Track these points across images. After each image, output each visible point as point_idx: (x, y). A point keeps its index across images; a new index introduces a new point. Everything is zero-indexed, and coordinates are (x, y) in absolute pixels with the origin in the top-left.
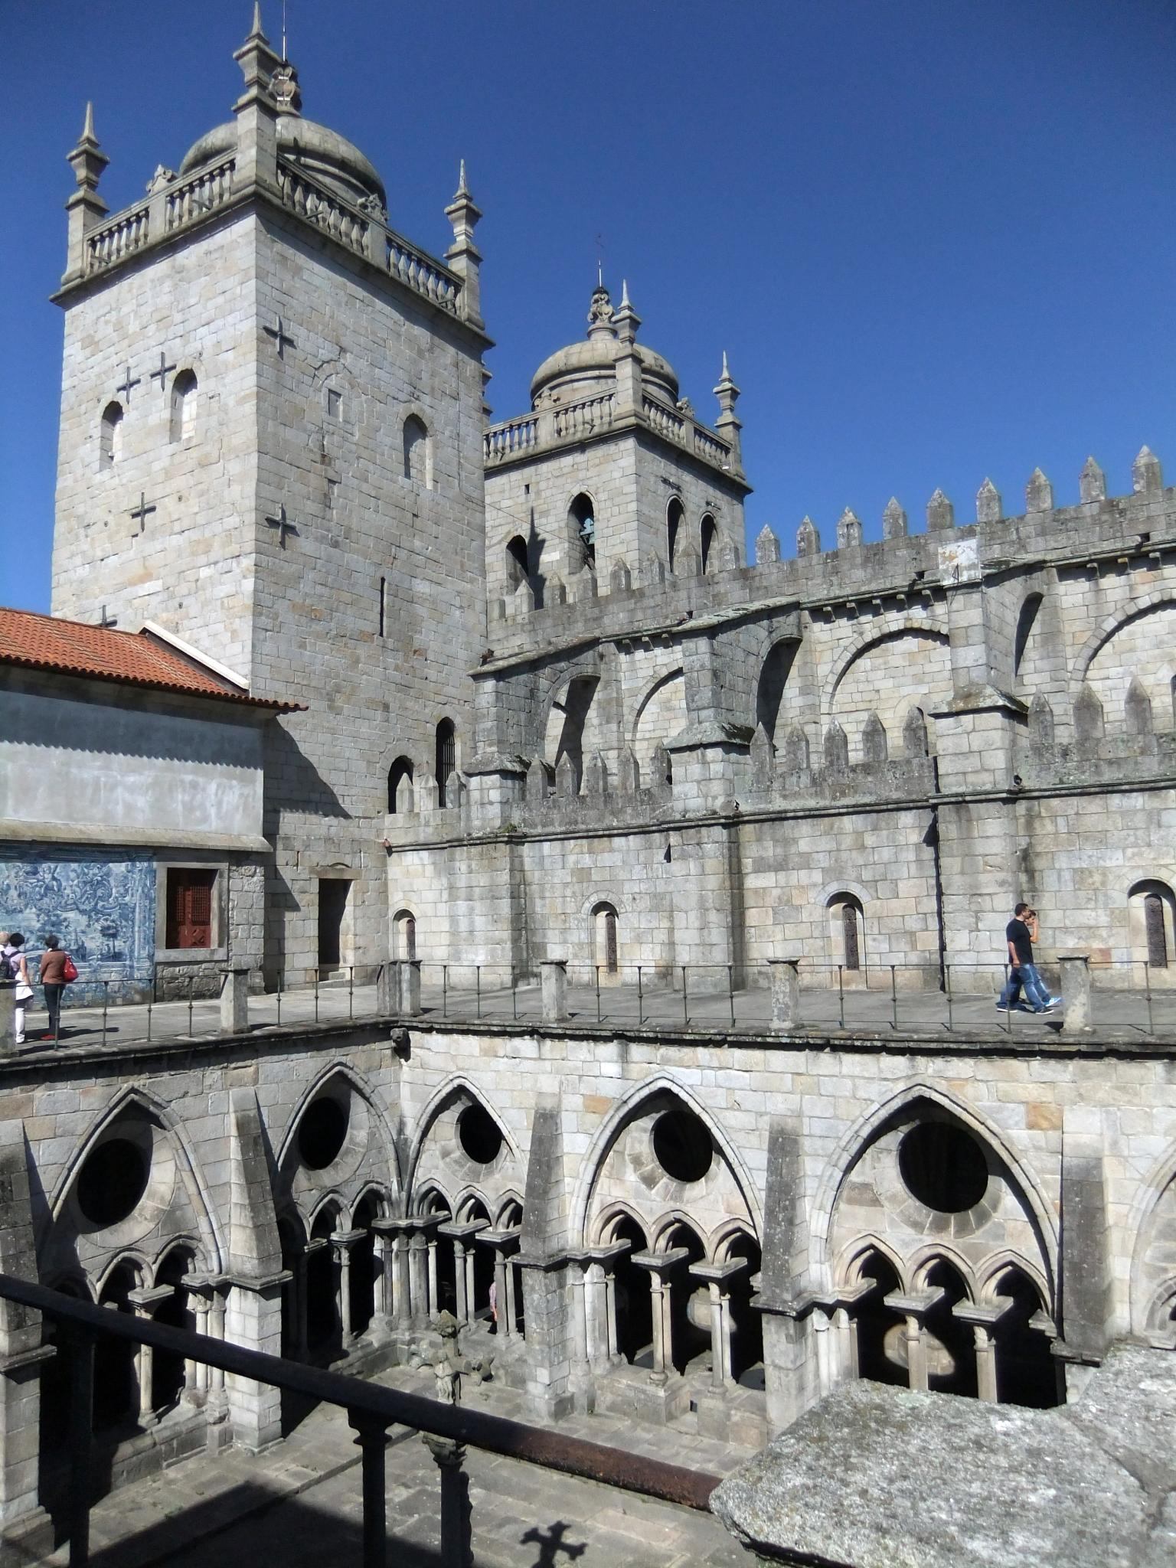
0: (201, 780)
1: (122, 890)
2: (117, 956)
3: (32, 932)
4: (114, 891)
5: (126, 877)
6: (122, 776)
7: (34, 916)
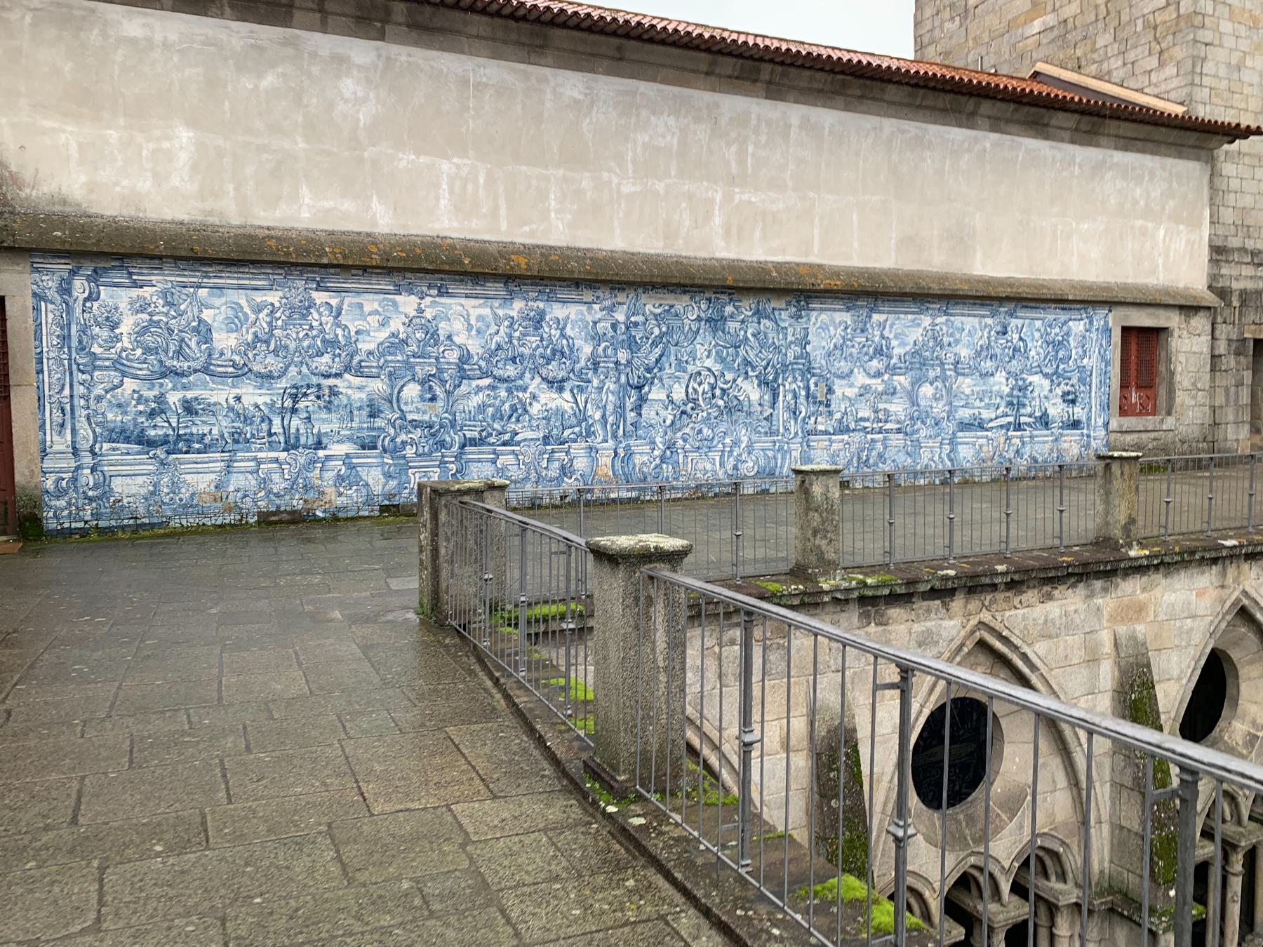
0: (1150, 225)
1: (1081, 353)
2: (1075, 424)
3: (1002, 398)
4: (1074, 352)
5: (1084, 337)
6: (1077, 223)
7: (1004, 380)
